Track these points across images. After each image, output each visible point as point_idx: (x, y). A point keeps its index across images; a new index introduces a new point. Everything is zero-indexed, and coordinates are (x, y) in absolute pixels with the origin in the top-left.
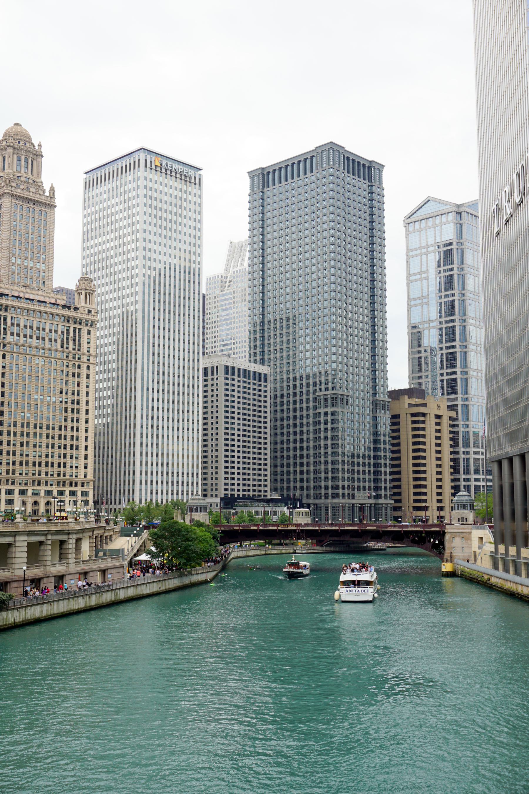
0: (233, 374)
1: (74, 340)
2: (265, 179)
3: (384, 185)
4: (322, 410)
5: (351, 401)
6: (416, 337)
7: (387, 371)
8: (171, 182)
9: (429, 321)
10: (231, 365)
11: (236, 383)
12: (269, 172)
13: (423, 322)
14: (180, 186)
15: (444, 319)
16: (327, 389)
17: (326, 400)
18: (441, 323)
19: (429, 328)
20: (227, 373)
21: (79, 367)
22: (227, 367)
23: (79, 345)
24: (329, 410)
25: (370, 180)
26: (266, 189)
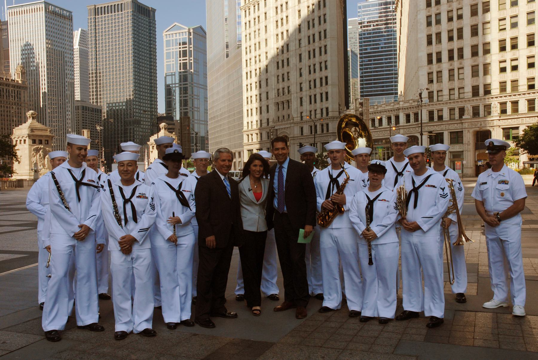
0: (86, 110)
1: (18, 96)
2: (97, 11)
3: (156, 19)
4: (129, 128)
5: (142, 123)
6: (169, 91)
7: (157, 109)
8: (58, 19)
9: (175, 84)
10: (84, 105)
11: (87, 114)
12: (98, 8)
13: (172, 84)
14: (62, 21)
15: (182, 83)
16: (130, 117)
17: (130, 122)
18: (181, 85)
19: (175, 87)
20: (83, 109)
21: (20, 109)
22: (83, 107)
23: (20, 98)
24: (132, 127)
25: (149, 17)
26: (97, 17)
